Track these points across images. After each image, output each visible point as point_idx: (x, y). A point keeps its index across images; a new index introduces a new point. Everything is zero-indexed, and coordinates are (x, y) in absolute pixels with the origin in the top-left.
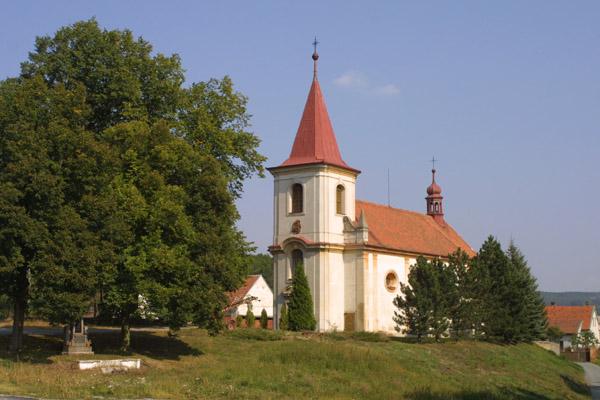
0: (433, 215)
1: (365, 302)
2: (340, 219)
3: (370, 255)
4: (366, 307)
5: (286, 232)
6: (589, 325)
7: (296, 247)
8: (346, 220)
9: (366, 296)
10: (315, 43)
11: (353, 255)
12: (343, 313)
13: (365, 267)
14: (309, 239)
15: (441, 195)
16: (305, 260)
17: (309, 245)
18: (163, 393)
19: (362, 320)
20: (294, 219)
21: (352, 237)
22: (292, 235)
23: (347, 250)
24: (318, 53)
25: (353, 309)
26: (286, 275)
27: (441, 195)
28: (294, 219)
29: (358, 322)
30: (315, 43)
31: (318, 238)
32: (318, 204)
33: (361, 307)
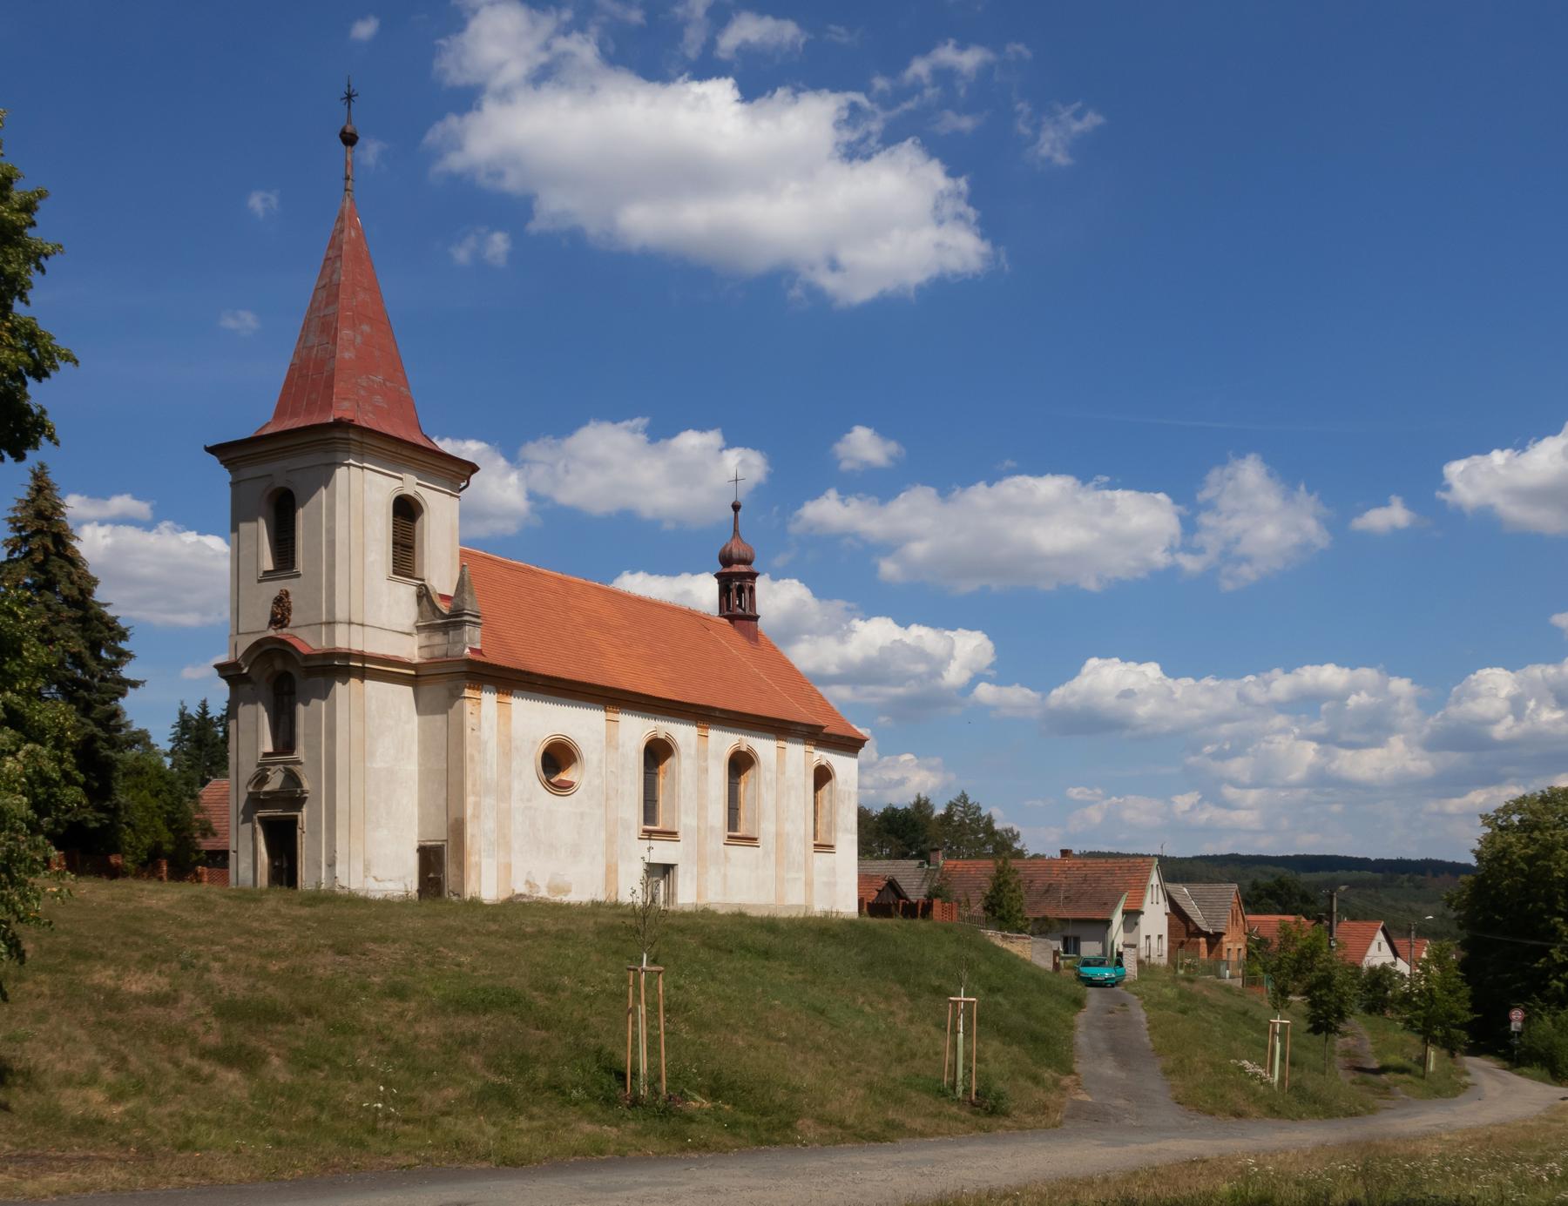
0: (732, 618)
1: (469, 812)
2: (405, 592)
3: (489, 699)
4: (470, 830)
5: (258, 624)
6: (1141, 900)
7: (279, 665)
8: (424, 595)
9: (470, 800)
10: (349, 97)
11: (437, 691)
12: (416, 845)
13: (340, 651)
14: (310, 641)
15: (754, 567)
16: (300, 708)
17: (307, 657)
18: (350, 1094)
19: (461, 865)
20: (274, 588)
21: (438, 639)
22: (272, 633)
23: (415, 677)
24: (356, 126)
25: (437, 835)
26: (257, 742)
27: (754, 567)
28: (274, 588)
29: (450, 870)
30: (349, 97)
31: (332, 636)
32: (332, 544)
33: (457, 829)
